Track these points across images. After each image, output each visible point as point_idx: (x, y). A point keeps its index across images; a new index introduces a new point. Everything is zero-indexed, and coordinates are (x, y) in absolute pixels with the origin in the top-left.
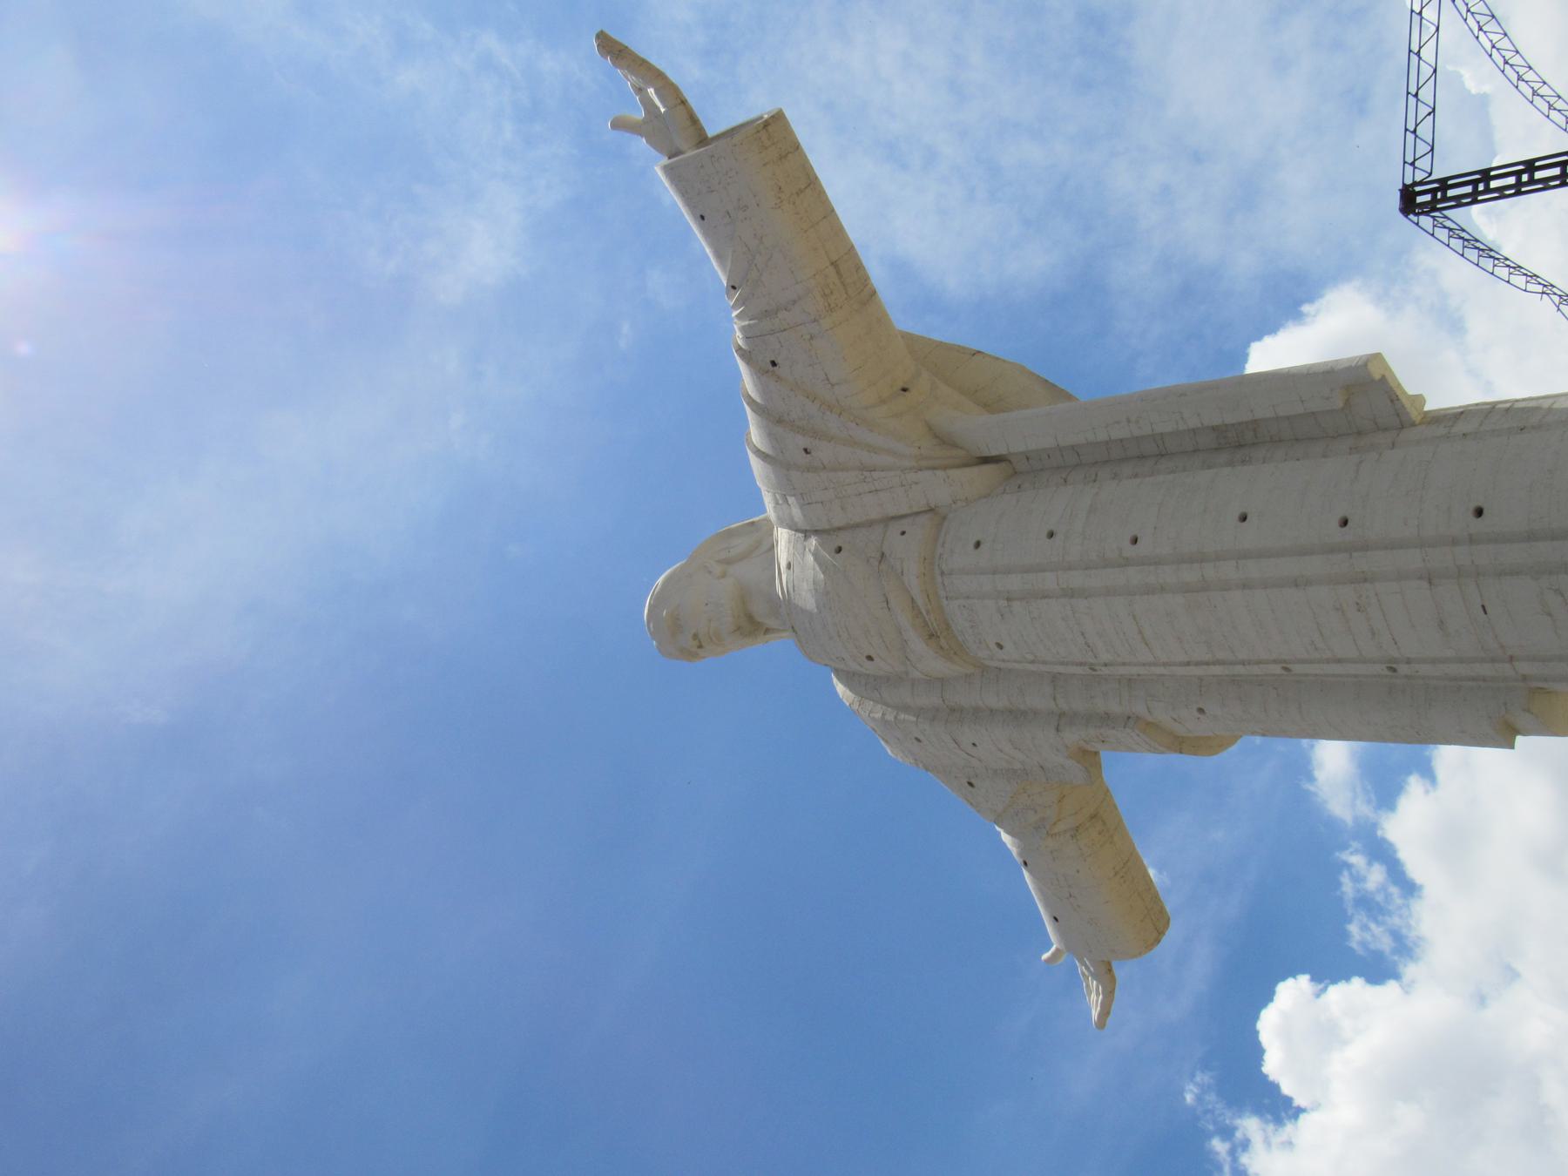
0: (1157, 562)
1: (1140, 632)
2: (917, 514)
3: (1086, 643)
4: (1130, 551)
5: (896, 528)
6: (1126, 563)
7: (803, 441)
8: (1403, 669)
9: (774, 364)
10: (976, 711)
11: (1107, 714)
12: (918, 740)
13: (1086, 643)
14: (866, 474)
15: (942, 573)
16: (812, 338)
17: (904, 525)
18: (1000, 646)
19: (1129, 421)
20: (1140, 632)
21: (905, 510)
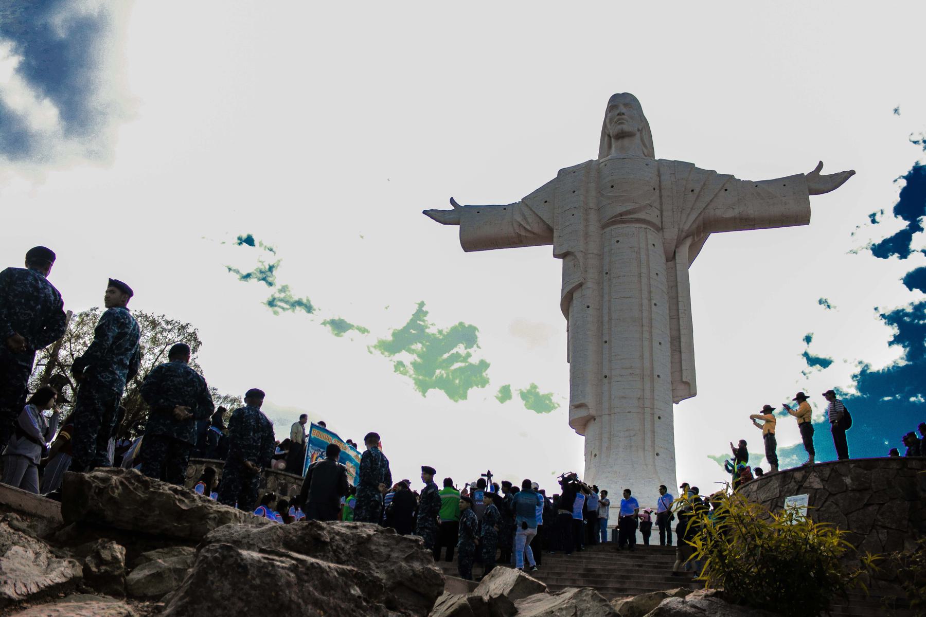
0: (650, 312)
1: (624, 297)
2: (662, 223)
3: (620, 276)
4: (653, 302)
5: (658, 213)
6: (650, 300)
7: (697, 191)
8: (606, 381)
9: (726, 190)
10: (587, 220)
11: (587, 271)
12: (574, 192)
13: (620, 276)
14: (680, 210)
15: (646, 229)
16: (733, 209)
17: (659, 216)
18: (618, 242)
19: (685, 310)
20: (624, 297)
21: (664, 219)
